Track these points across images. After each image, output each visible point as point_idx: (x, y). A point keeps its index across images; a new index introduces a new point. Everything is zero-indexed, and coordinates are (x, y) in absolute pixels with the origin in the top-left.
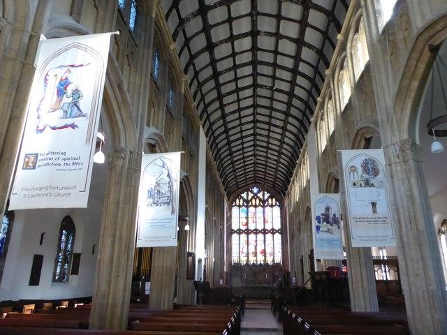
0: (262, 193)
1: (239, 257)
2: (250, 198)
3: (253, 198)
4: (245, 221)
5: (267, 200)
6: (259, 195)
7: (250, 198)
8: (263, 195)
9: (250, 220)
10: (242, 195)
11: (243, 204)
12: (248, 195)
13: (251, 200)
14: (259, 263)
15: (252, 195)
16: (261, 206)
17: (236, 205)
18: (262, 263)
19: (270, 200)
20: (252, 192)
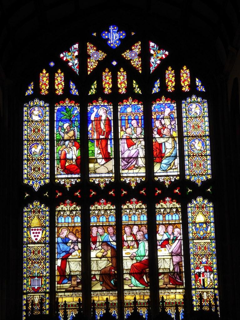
0: (137, 49)
1: (53, 293)
2: (92, 64)
3: (102, 65)
4: (73, 153)
5: (160, 72)
6: (127, 55)
7: (92, 64)
8: (145, 55)
9: (95, 150)
10: (65, 56)
11: (67, 89)
12: (83, 57)
13: (97, 75)
14: (128, 312)
15: (101, 55)
16: (136, 97)
17: (37, 94)
18: (143, 312)
19: (170, 75)
20: (102, 45)
